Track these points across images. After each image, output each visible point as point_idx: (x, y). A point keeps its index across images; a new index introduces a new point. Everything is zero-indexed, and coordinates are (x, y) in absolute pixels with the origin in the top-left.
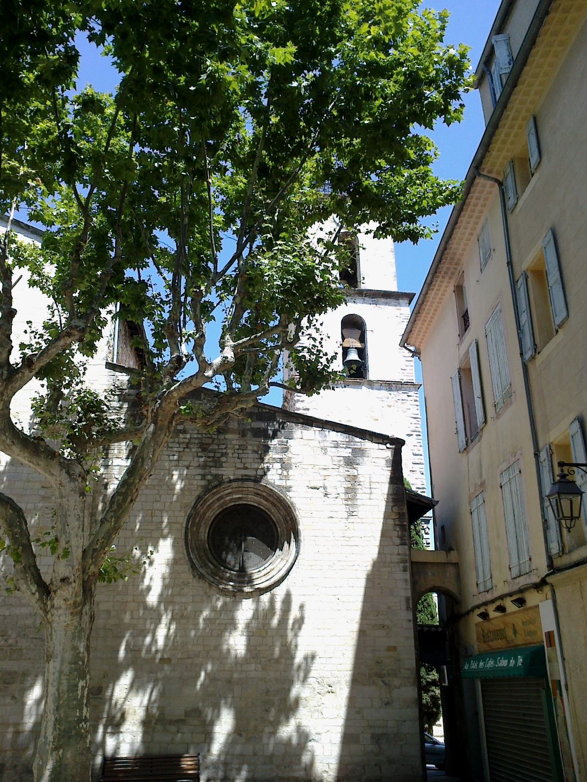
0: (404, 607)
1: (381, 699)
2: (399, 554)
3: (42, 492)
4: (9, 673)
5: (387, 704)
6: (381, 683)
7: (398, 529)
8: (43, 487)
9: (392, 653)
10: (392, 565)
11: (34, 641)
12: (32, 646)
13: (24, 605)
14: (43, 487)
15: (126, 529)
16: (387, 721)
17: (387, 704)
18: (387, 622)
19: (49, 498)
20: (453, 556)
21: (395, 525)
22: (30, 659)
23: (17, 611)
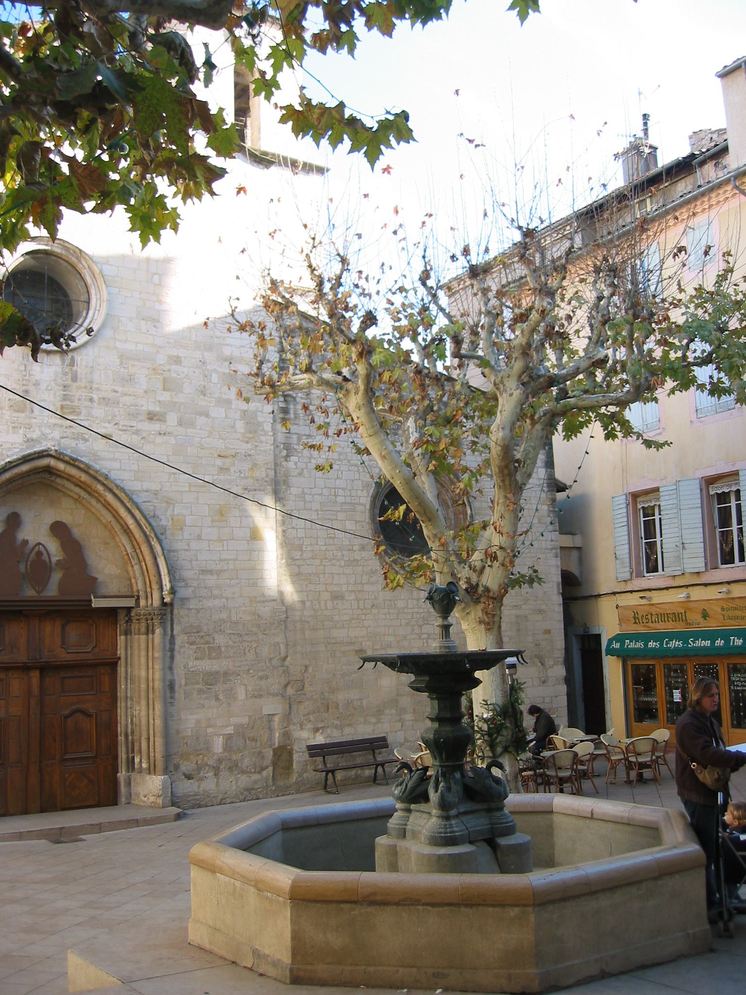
0: (555, 592)
1: (540, 679)
2: (552, 541)
3: (219, 462)
4: (210, 674)
5: (544, 682)
6: (539, 664)
7: (551, 515)
8: (219, 456)
9: (547, 636)
10: (546, 551)
11: (232, 636)
12: (231, 643)
13: (216, 597)
14: (219, 456)
15: (311, 510)
16: (544, 698)
17: (544, 682)
18: (544, 607)
19: (228, 470)
20: (577, 541)
21: (550, 511)
22: (230, 657)
23: (209, 603)
